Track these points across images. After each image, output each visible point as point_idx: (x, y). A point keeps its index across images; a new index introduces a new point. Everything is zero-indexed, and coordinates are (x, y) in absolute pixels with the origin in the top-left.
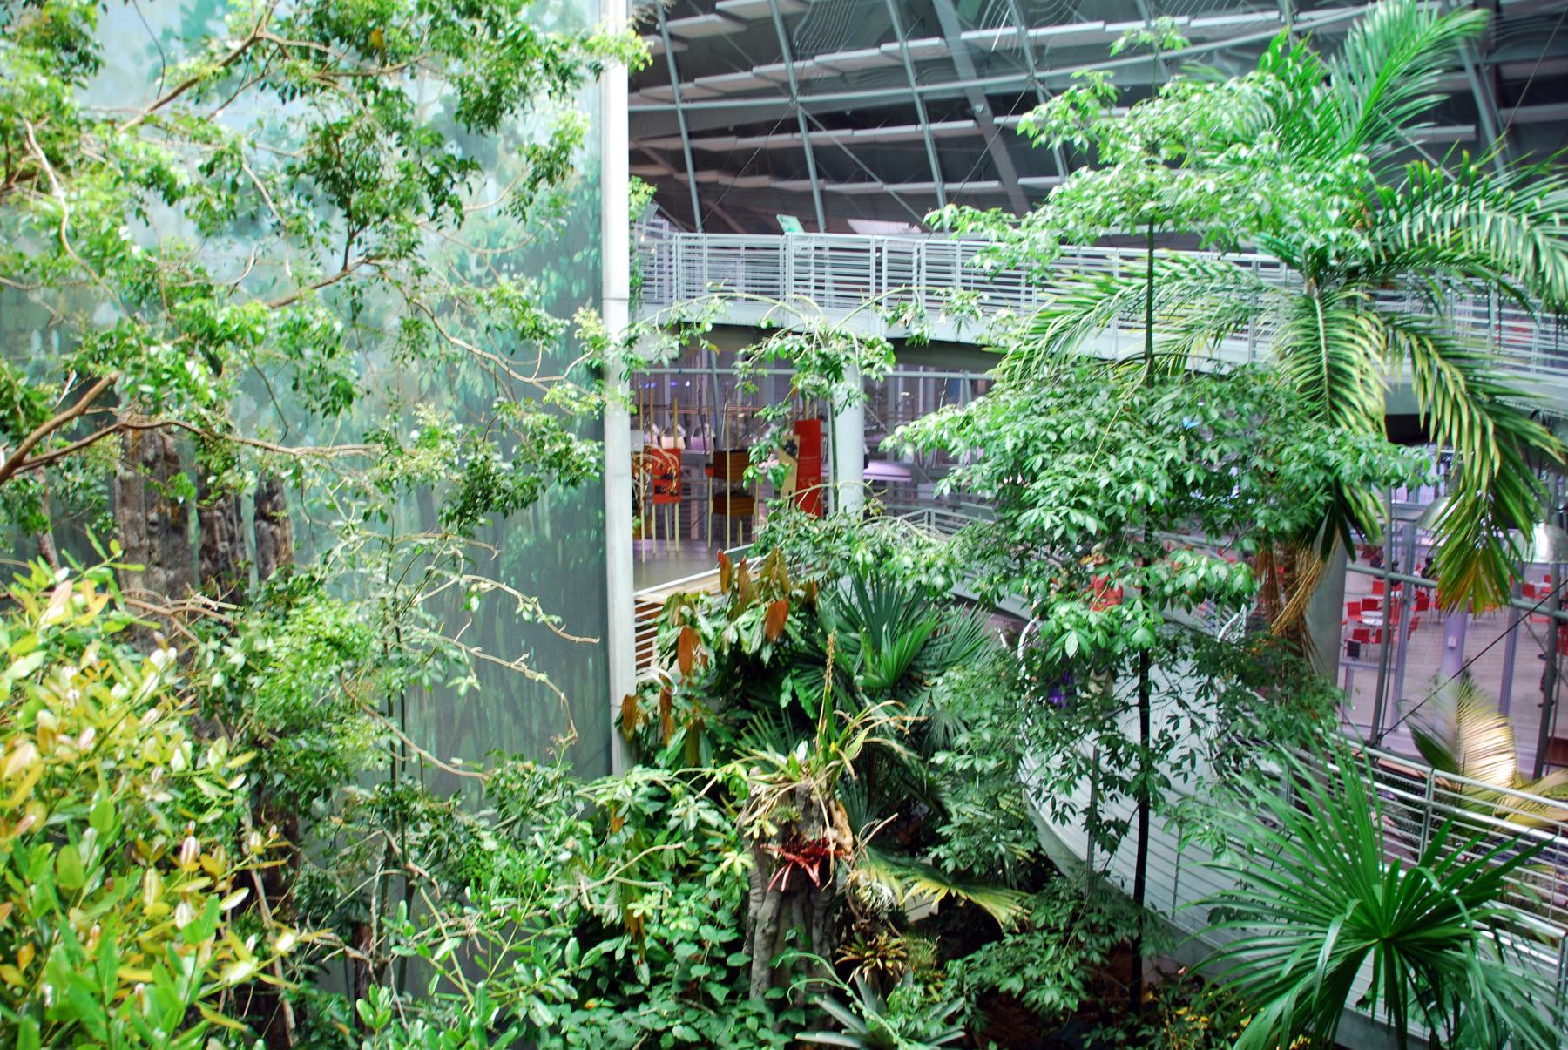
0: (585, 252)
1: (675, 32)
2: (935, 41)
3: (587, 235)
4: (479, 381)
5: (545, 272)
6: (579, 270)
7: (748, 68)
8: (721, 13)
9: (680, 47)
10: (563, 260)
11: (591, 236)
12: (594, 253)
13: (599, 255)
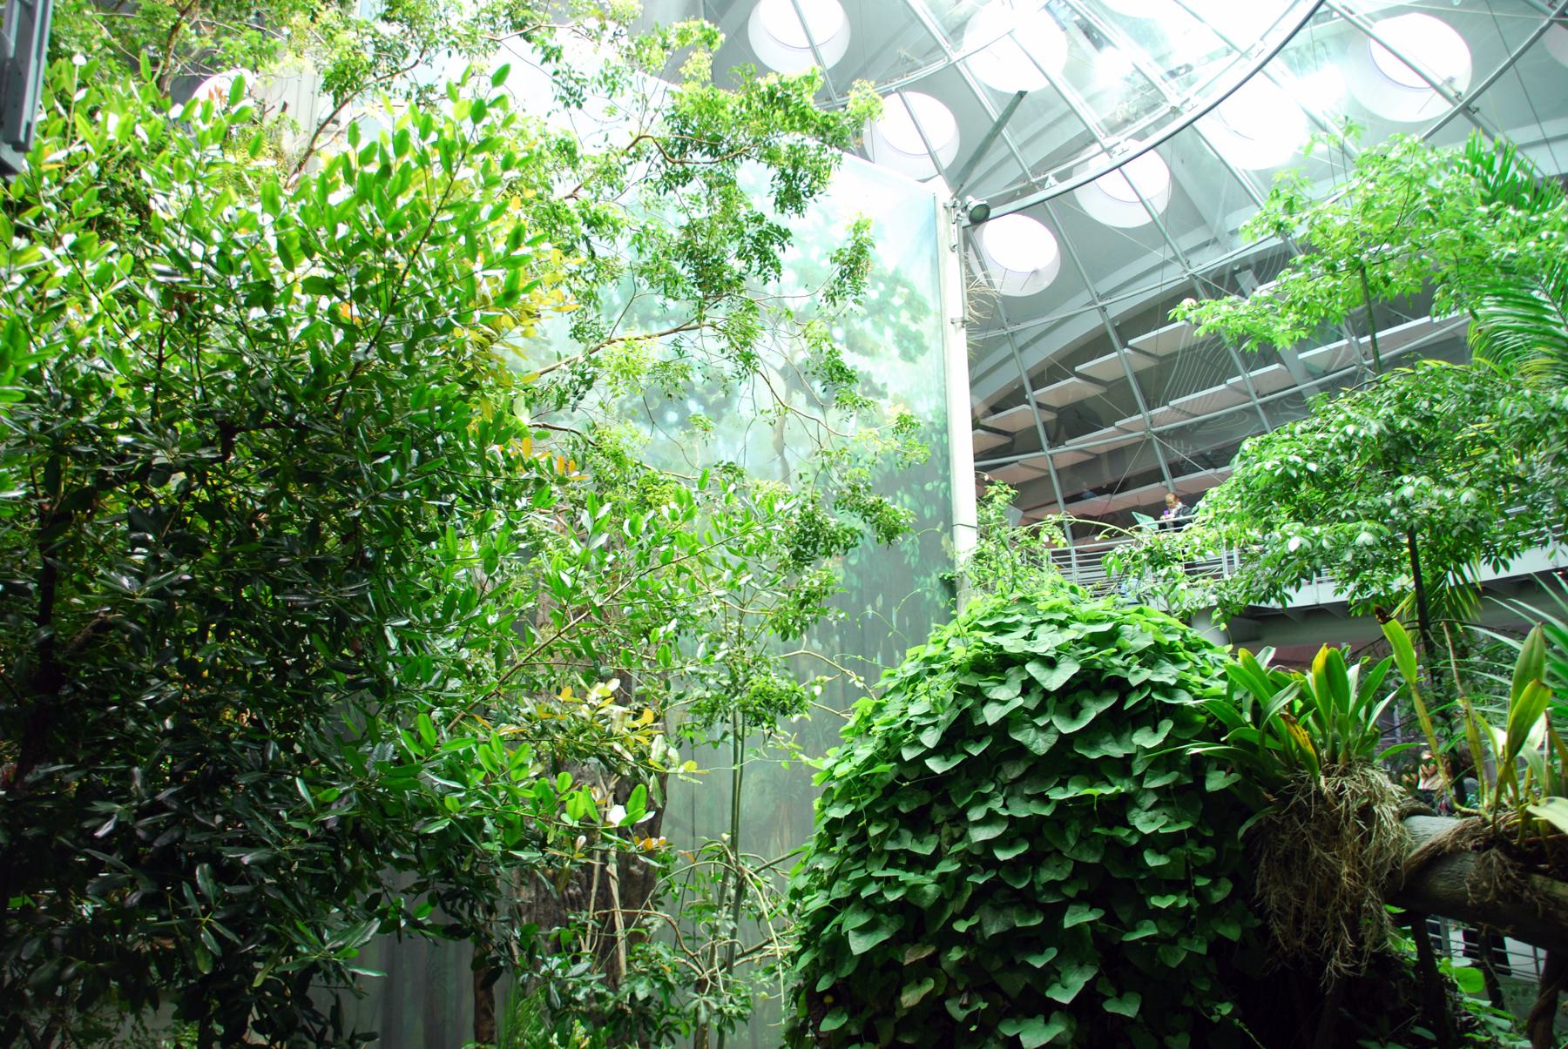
1: (1042, 401)
2: (1276, 366)
4: (841, 571)
6: (930, 498)
8: (1079, 375)
9: (1050, 416)
10: (915, 486)
12: (943, 485)
13: (948, 488)
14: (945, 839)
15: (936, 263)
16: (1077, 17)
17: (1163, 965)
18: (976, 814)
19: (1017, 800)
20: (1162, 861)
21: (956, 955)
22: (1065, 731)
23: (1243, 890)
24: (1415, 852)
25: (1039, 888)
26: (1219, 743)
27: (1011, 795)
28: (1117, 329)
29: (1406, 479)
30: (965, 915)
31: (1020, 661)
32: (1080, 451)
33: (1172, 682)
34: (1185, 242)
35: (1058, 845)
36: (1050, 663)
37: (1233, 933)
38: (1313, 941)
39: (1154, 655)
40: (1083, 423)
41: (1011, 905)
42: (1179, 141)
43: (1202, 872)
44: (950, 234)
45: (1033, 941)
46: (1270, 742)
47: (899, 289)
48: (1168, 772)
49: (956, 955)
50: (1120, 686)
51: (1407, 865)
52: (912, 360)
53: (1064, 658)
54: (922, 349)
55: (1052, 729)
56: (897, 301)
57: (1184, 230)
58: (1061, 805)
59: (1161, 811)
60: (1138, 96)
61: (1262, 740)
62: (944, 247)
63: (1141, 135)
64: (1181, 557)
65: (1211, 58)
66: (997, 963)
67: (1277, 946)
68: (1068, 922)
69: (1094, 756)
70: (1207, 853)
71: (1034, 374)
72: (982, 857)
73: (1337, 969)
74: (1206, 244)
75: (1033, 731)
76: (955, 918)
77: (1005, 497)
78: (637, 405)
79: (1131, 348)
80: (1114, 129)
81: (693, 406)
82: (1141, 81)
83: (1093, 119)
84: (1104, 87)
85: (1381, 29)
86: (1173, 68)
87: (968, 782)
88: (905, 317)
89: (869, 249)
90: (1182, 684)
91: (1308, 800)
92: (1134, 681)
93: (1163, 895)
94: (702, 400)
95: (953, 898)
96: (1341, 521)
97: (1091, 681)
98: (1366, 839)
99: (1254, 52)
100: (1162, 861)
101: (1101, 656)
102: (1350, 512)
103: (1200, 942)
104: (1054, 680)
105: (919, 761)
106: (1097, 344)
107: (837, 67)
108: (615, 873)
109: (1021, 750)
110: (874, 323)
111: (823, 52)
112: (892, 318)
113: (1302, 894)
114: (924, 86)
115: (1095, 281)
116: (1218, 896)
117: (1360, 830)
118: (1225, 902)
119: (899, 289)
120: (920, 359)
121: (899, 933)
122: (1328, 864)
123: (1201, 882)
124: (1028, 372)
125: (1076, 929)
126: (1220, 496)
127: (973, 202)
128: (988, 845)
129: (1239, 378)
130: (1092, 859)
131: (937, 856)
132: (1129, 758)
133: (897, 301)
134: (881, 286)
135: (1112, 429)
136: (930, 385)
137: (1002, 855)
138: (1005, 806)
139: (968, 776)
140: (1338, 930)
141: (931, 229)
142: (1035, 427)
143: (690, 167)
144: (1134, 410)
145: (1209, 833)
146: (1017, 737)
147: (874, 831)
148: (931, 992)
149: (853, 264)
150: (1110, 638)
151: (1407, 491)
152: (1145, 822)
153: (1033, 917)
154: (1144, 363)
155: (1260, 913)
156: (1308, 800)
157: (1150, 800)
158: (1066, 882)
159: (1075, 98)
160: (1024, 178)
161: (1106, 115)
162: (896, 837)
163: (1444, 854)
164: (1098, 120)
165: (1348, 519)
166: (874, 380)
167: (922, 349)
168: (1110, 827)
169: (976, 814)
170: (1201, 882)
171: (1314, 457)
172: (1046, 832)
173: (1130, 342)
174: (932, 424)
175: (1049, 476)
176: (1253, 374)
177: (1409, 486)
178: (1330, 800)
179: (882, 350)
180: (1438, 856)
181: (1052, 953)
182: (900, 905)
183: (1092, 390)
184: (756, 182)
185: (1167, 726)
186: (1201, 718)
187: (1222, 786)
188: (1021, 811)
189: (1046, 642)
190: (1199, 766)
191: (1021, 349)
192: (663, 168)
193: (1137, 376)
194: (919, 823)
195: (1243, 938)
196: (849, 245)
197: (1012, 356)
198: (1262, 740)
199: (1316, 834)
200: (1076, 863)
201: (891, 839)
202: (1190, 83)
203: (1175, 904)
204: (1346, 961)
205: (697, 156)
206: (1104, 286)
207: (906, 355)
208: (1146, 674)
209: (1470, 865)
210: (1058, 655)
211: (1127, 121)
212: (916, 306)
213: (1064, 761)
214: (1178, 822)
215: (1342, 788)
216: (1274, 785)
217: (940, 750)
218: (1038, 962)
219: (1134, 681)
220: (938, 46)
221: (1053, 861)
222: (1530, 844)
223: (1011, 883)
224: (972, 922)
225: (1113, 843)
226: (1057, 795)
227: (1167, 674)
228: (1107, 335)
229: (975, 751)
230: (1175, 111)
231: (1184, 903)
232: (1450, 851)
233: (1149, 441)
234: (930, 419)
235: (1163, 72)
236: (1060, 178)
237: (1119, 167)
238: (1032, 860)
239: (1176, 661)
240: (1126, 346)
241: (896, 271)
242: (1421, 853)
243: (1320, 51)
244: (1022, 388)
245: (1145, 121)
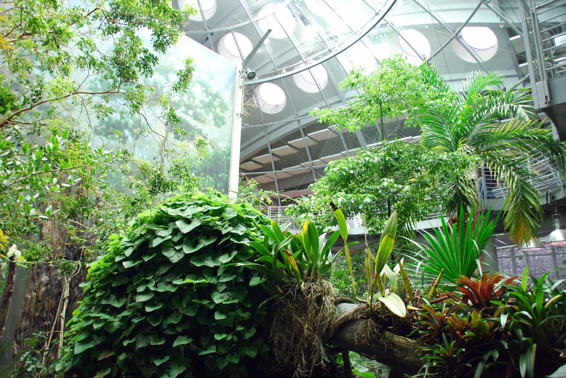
0: (223, 174)
3: (224, 169)
5: (208, 176)
6: (220, 180)
7: (299, 164)
8: (289, 145)
9: (276, 159)
11: (225, 170)
12: (226, 175)
13: (228, 177)
14: (129, 301)
15: (233, 92)
16: (299, 13)
17: (217, 368)
18: (141, 289)
19: (162, 284)
20: (223, 317)
21: (122, 357)
22: (186, 253)
23: (262, 333)
25: (165, 327)
26: (253, 262)
27: (161, 281)
28: (304, 129)
29: (385, 179)
30: (130, 338)
31: (173, 219)
32: (285, 172)
33: (241, 234)
34: (331, 101)
35: (177, 307)
36: (188, 221)
37: (253, 354)
38: (292, 359)
39: (236, 221)
40: (281, 156)
41: (151, 334)
42: (330, 61)
43: (241, 324)
44: (240, 82)
45: (159, 352)
46: (279, 264)
47: (217, 99)
48: (232, 275)
49: (122, 357)
50: (218, 234)
51: (334, 326)
52: (219, 127)
53: (195, 219)
54: (224, 123)
55: (182, 252)
56: (216, 104)
57: (331, 96)
58: (180, 287)
59: (226, 294)
60: (318, 45)
61: (275, 262)
62: (237, 87)
63: (316, 59)
64: (312, 210)
65: (345, 34)
66: (142, 362)
67: (277, 362)
68: (175, 344)
69: (199, 265)
70: (246, 315)
71: (272, 143)
72: (140, 311)
73: (299, 373)
74: (339, 102)
75: (174, 252)
76: (125, 339)
77: (254, 185)
78: (102, 129)
79: (308, 137)
80: (309, 55)
81: (127, 132)
82: (320, 40)
83: (302, 51)
84: (307, 40)
85: (403, 33)
86: (331, 36)
87: (143, 274)
88: (218, 110)
89: (193, 72)
90: (246, 236)
91: (294, 292)
92: (224, 232)
93: (221, 334)
94: (131, 130)
95: (126, 329)
96: (360, 193)
97: (205, 230)
98: (317, 312)
99: (359, 33)
100: (223, 317)
101: (215, 220)
102: (364, 191)
103: (236, 357)
104: (186, 229)
105: (120, 262)
106: (296, 134)
107: (209, 20)
108: (64, 317)
109: (167, 261)
110: (206, 111)
111: (205, 13)
112: (213, 110)
113: (289, 336)
114: (241, 30)
115: (297, 112)
116: (248, 336)
117: (315, 308)
118: (251, 339)
119: (217, 99)
120: (222, 127)
121: (102, 344)
122: (299, 323)
123: (240, 328)
124: (270, 142)
125: (178, 347)
126: (320, 185)
127: (249, 71)
128: (145, 304)
129: (345, 152)
130: (191, 314)
131: (123, 308)
132: (216, 268)
133: (216, 104)
134: (210, 97)
135: (299, 166)
136: (227, 138)
137: (148, 309)
138: (156, 286)
139: (144, 271)
140: (301, 354)
141: (233, 79)
142: (271, 163)
143: (119, 25)
144: (307, 160)
145: (249, 306)
146: (165, 254)
147: (98, 294)
148: (109, 374)
149: (185, 77)
150: (219, 212)
151: (385, 184)
152: (218, 299)
153: (161, 341)
154: (312, 143)
155: (271, 345)
156: (294, 292)
157: (224, 287)
158: (178, 325)
159: (296, 43)
160: (275, 69)
161: (307, 50)
162: (108, 298)
163: (349, 320)
164: (304, 52)
165: (363, 193)
166: (203, 132)
167: (224, 123)
168: (201, 299)
169: (141, 289)
170: (240, 328)
171: (353, 169)
172: (172, 300)
173: (308, 135)
174: (224, 152)
175: (274, 182)
176: (350, 151)
177: (386, 182)
178: (304, 293)
179: (207, 121)
180: (348, 322)
181: (167, 358)
182: (98, 332)
183: (294, 151)
184: (145, 35)
185: (235, 253)
186: (251, 251)
187: (257, 284)
188: (162, 289)
189: (189, 212)
190: (248, 273)
191: (268, 134)
192: (107, 25)
193: (310, 148)
194: (120, 292)
195: (258, 356)
196: (185, 69)
197: (264, 136)
198: (275, 262)
199: (296, 309)
200: (185, 316)
201: (105, 299)
202: (336, 42)
203: (226, 338)
204: (303, 370)
205: (122, 21)
206: (301, 113)
207: (217, 124)
208: (230, 229)
209: (360, 326)
210: (193, 218)
211: (313, 53)
212: (224, 107)
213: (184, 267)
214: (233, 299)
215: (310, 288)
216: (282, 284)
217: (132, 258)
218: (158, 363)
219: (224, 232)
220: (248, 16)
221: (175, 315)
222: (386, 317)
223: (151, 323)
224: (131, 342)
225: (202, 307)
226: (178, 282)
227: (241, 230)
228: (299, 131)
229: (146, 259)
230: (330, 51)
231: (229, 338)
232: (351, 319)
233: (311, 172)
234: (224, 149)
235: (328, 37)
236: (287, 70)
237: (308, 69)
238: (166, 313)
239: (249, 226)
240: (306, 135)
241: (217, 93)
242: (341, 320)
243: (381, 36)
244: (268, 148)
245: (320, 53)
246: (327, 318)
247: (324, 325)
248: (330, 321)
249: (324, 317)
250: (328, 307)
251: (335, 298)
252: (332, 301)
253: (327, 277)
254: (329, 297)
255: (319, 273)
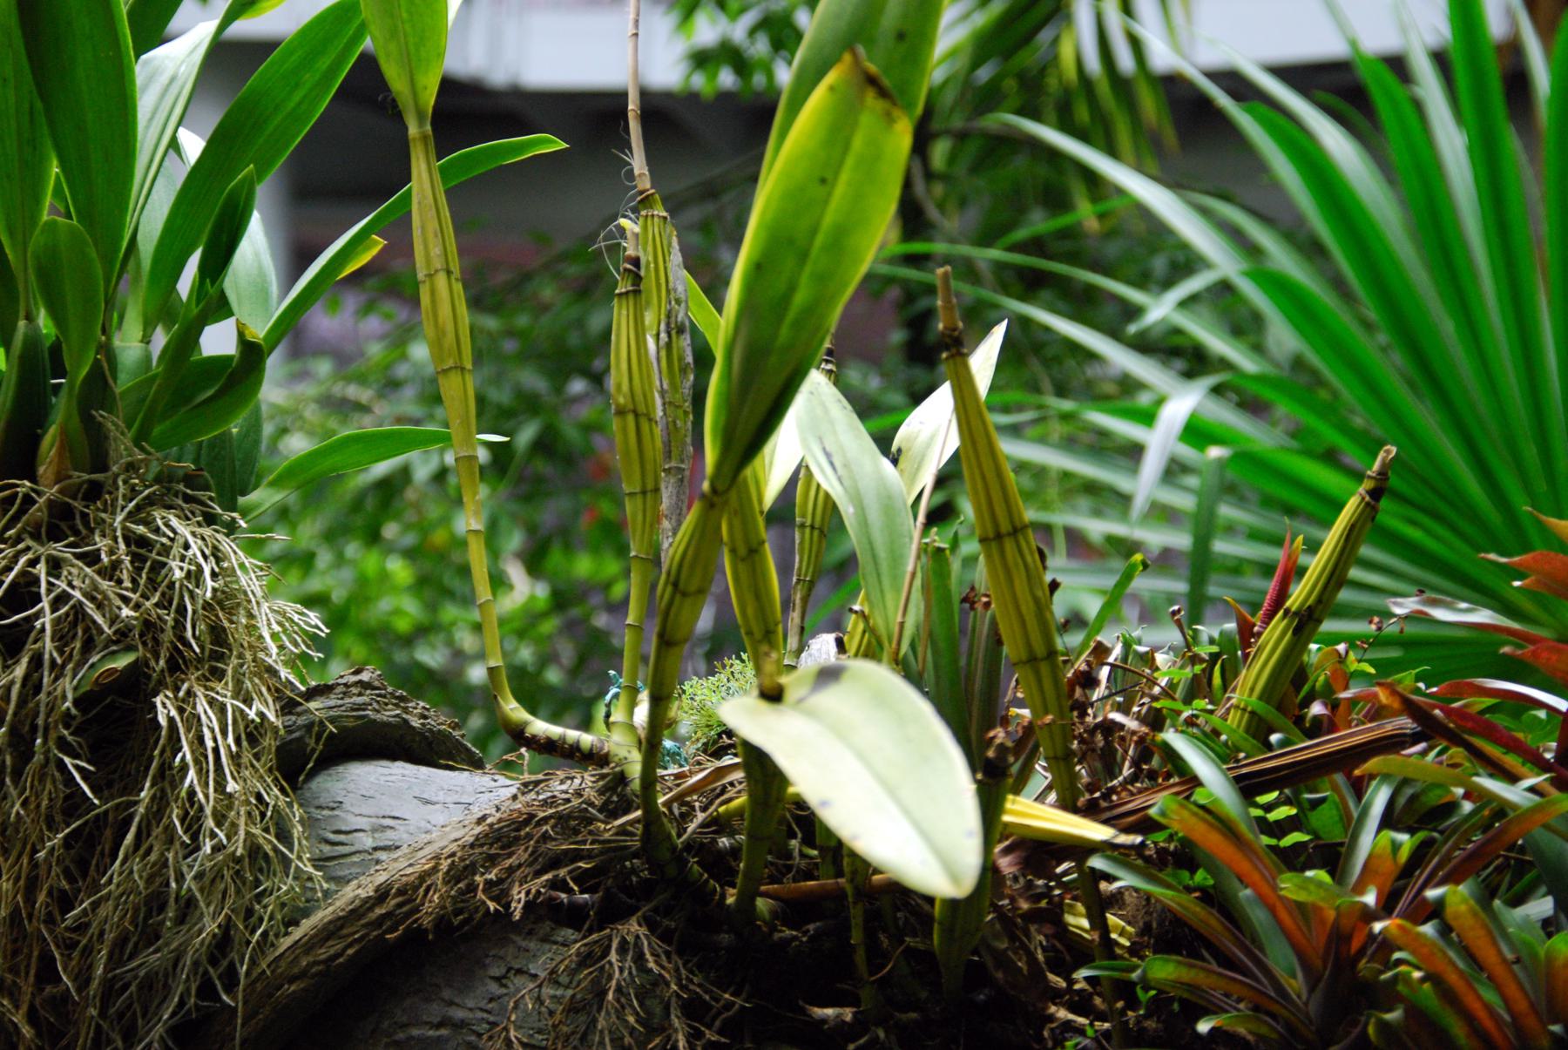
24: (306, 926)
98: (90, 849)
117: (74, 803)
163: (416, 936)
222: (795, 910)
232: (442, 923)
246: (188, 906)
247: (155, 986)
248: (223, 942)
249: (156, 901)
250: (208, 799)
251: (289, 708)
252: (252, 734)
253: (216, 484)
254: (224, 692)
255: (122, 447)
